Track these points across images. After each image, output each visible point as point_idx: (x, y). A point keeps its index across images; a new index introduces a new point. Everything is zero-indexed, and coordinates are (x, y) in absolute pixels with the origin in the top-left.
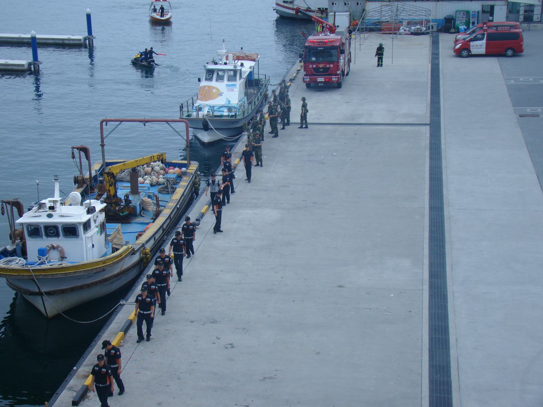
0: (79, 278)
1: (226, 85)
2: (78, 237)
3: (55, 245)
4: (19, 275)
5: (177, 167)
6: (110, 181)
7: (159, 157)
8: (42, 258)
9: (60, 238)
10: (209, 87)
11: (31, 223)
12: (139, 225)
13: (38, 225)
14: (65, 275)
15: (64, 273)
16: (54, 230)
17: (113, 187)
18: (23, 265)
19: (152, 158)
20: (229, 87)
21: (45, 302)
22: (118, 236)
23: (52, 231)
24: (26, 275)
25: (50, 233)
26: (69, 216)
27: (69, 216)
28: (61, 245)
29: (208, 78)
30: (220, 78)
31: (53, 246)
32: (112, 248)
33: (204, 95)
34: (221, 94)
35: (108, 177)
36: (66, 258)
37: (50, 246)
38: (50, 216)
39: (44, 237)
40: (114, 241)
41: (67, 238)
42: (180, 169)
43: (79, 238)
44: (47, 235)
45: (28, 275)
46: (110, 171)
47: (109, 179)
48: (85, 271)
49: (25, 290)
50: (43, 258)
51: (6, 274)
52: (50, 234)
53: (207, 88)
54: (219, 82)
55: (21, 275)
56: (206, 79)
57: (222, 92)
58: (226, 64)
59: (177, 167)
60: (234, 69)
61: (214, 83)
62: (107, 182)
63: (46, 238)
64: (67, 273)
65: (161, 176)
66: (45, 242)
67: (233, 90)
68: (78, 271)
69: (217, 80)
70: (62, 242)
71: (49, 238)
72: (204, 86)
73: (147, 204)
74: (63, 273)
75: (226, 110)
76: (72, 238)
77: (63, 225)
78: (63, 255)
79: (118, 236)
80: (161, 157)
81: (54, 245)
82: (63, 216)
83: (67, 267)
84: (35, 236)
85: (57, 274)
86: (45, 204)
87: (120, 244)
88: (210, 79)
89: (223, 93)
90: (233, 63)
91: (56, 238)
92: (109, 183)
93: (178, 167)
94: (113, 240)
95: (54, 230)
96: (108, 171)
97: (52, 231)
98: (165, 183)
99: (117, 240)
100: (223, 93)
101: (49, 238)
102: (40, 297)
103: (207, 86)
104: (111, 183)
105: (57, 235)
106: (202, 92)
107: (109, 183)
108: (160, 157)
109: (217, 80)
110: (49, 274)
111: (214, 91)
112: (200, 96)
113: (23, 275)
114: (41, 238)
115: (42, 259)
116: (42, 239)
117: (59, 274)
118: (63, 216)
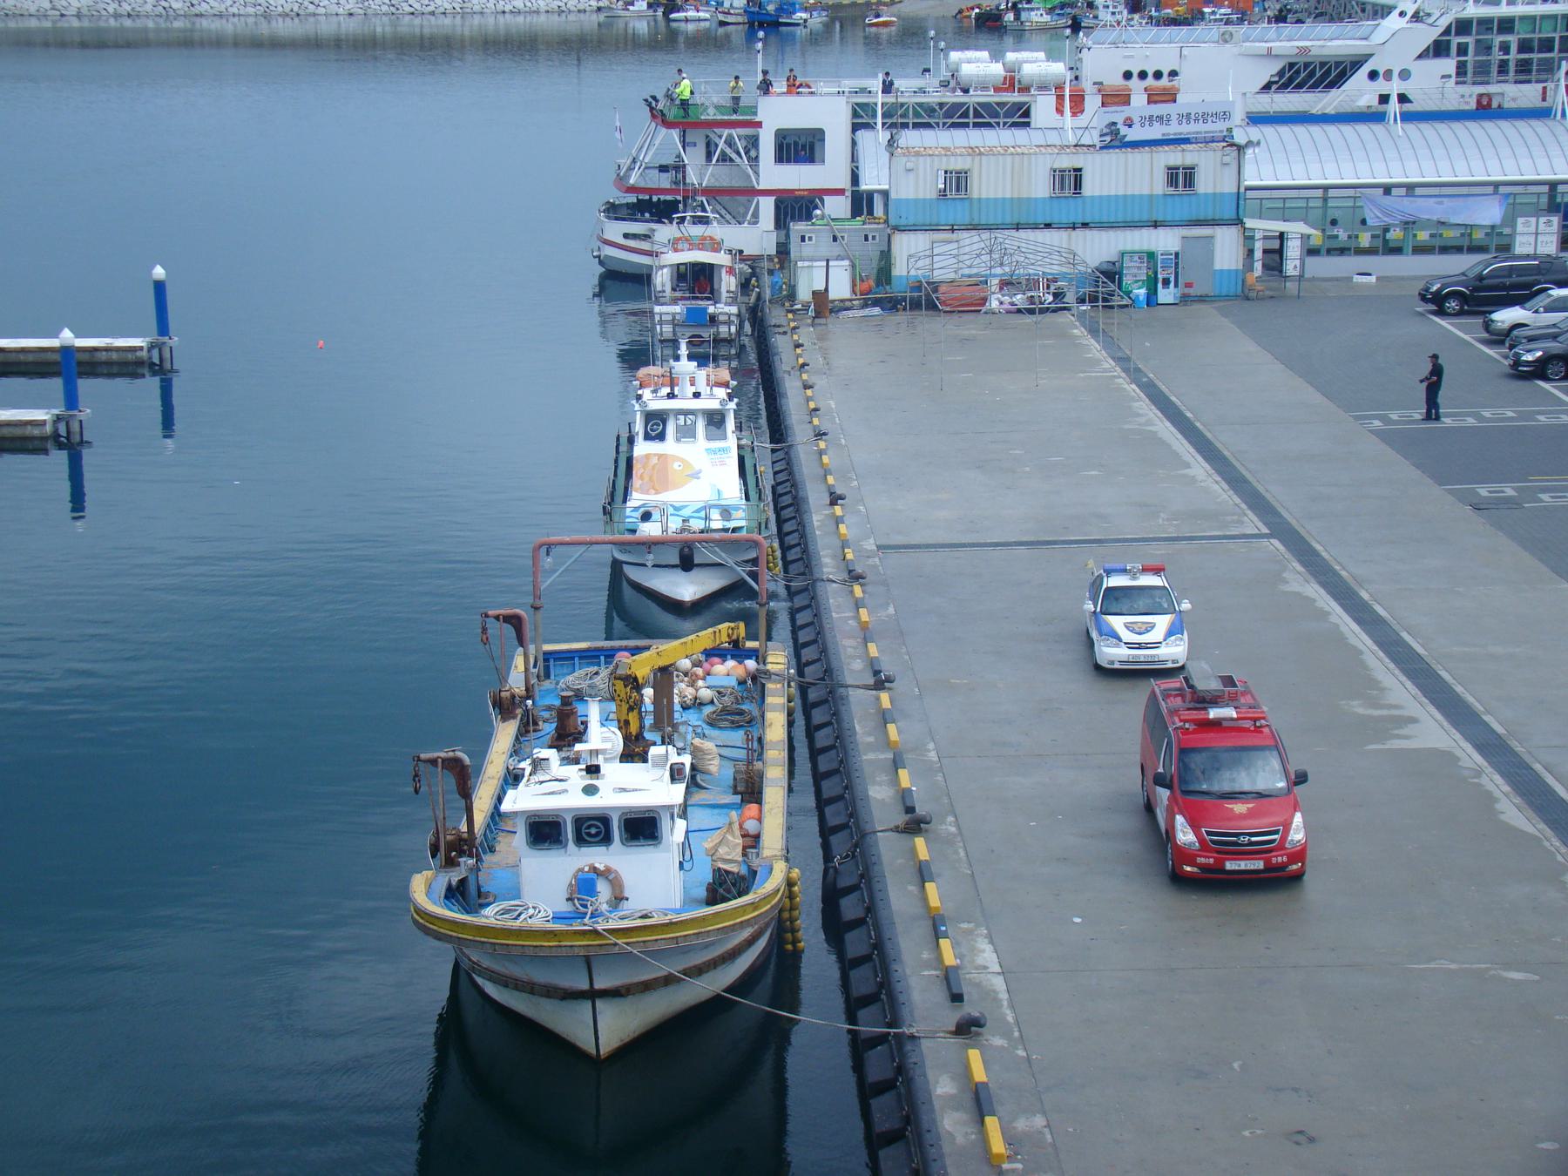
0: (706, 946)
1: (707, 450)
2: (660, 843)
3: (601, 867)
4: (560, 946)
5: (729, 657)
6: (630, 697)
7: (730, 631)
8: (588, 901)
9: (612, 847)
10: (660, 456)
11: (538, 811)
12: (708, 811)
13: (557, 816)
14: (675, 941)
15: (673, 938)
16: (597, 827)
17: (636, 711)
18: (548, 921)
19: (717, 634)
20: (713, 456)
21: (599, 1018)
22: (730, 838)
23: (593, 831)
24: (580, 946)
25: (589, 834)
26: (640, 790)
27: (640, 790)
28: (614, 866)
29: (653, 434)
30: (687, 433)
31: (595, 868)
32: (714, 870)
33: (651, 477)
34: (695, 475)
35: (626, 686)
36: (627, 899)
37: (586, 869)
38: (590, 790)
39: (571, 844)
40: (722, 851)
41: (631, 846)
42: (740, 663)
43: (661, 846)
44: (581, 840)
45: (584, 946)
46: (629, 673)
47: (627, 693)
48: (718, 929)
49: (545, 986)
50: (593, 899)
51: (523, 946)
52: (588, 839)
53: (655, 460)
54: (685, 442)
55: (565, 946)
56: (647, 437)
57: (697, 468)
58: (697, 395)
59: (729, 657)
60: (720, 407)
61: (670, 446)
62: (621, 701)
63: (577, 849)
64: (680, 936)
65: (700, 683)
66: (570, 861)
67: (723, 464)
68: (703, 930)
69: (678, 440)
70: (618, 857)
71: (585, 850)
72: (648, 456)
73: (705, 756)
74: (669, 938)
75: (715, 514)
76: (643, 846)
77: (623, 813)
78: (622, 892)
79: (730, 838)
80: (735, 631)
81: (597, 865)
82: (624, 790)
83: (681, 921)
84: (547, 844)
85: (656, 940)
86: (547, 759)
87: (735, 858)
88: (661, 437)
89: (700, 471)
90: (709, 393)
91: (603, 849)
92: (628, 702)
93: (732, 658)
94: (717, 850)
95: (597, 827)
96: (624, 672)
97: (593, 831)
98: (715, 700)
99: (726, 849)
100: (700, 471)
101: (582, 849)
102: (588, 1004)
103: (655, 455)
104: (632, 704)
105: (606, 839)
106: (642, 471)
107: (628, 702)
108: (733, 634)
109: (678, 440)
110: (638, 942)
111: (676, 465)
112: (640, 482)
113: (571, 946)
114: (563, 850)
115: (589, 903)
116: (566, 852)
117: (661, 939)
118: (624, 790)
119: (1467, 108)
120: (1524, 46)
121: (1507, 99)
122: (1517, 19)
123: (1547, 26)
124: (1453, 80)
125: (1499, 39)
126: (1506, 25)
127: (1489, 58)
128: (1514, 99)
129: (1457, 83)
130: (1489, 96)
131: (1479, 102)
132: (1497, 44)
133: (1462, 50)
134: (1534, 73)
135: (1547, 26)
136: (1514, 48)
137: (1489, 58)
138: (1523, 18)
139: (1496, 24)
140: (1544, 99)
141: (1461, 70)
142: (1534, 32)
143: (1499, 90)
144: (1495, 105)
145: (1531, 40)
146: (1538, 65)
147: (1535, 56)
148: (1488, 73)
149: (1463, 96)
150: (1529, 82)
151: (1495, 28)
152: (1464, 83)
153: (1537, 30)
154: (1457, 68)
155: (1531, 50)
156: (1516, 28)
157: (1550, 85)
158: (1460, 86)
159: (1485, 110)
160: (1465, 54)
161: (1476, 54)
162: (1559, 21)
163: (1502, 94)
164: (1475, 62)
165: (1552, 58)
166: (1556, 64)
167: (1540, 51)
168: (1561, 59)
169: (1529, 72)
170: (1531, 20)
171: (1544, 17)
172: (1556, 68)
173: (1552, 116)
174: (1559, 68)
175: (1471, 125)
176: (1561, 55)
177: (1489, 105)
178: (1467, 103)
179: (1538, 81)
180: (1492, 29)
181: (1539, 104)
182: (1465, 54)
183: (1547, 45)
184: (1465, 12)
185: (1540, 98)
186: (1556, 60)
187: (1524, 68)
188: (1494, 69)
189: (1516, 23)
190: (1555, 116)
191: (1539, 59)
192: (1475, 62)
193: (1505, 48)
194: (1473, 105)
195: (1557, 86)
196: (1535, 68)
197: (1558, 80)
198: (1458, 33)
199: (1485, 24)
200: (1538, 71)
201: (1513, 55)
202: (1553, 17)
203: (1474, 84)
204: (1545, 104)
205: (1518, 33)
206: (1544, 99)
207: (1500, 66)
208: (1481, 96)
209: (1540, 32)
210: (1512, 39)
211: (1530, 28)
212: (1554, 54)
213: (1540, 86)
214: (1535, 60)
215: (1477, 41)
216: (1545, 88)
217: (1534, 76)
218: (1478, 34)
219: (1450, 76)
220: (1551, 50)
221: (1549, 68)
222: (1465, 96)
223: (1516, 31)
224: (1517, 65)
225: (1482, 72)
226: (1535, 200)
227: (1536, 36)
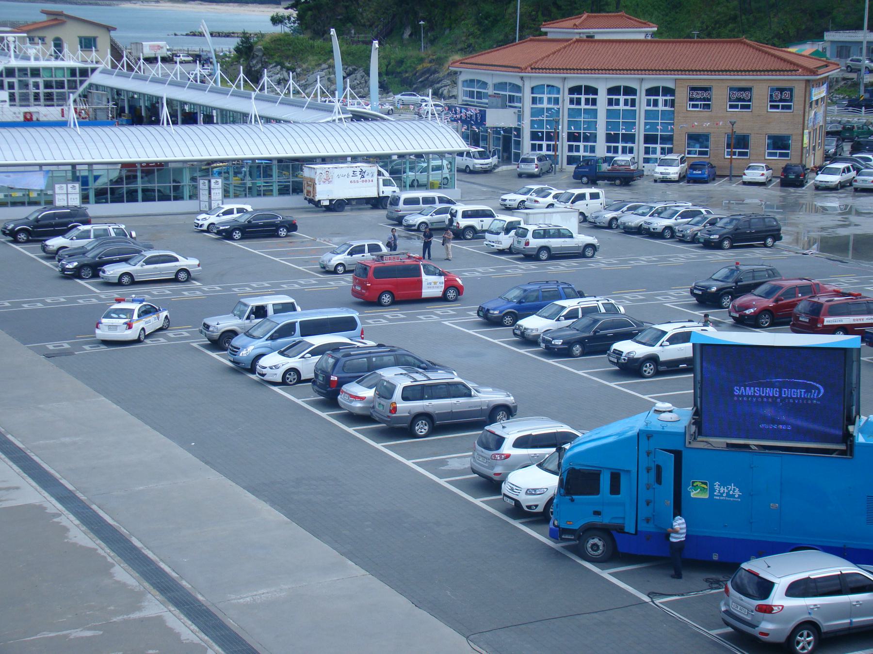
119: (18, 120)
120: (48, 85)
121: (41, 115)
122: (41, 69)
123: (59, 73)
124: (8, 103)
125: (31, 80)
126: (36, 72)
127: (28, 91)
128: (45, 116)
129: (11, 105)
130: (30, 113)
131: (25, 117)
132: (31, 83)
133: (11, 86)
134: (55, 100)
135: (59, 73)
136: (42, 86)
137: (28, 91)
138: (45, 69)
139: (29, 71)
140: (63, 116)
141: (12, 97)
142: (52, 76)
143: (36, 110)
144: (34, 118)
145: (51, 82)
146: (57, 96)
147: (54, 91)
148: (28, 100)
149: (15, 113)
150: (53, 106)
151: (29, 74)
152: (15, 105)
153: (54, 76)
154: (10, 96)
155: (52, 87)
156: (41, 74)
157: (65, 108)
158: (12, 107)
159: (29, 121)
160: (13, 88)
161: (20, 88)
162: (65, 71)
163: (38, 113)
164: (20, 93)
165: (65, 92)
166: (67, 95)
167: (57, 88)
168: (69, 93)
169: (52, 100)
170: (49, 69)
171: (57, 69)
172: (67, 98)
173: (68, 126)
174: (69, 98)
175: (21, 130)
176: (69, 91)
177: (31, 119)
178: (18, 117)
179: (58, 105)
180: (27, 74)
181: (60, 118)
182: (13, 88)
183: (60, 85)
184: (10, 64)
185: (60, 115)
186: (67, 93)
187: (49, 97)
188: (32, 98)
189: (41, 71)
190: (70, 125)
191: (57, 93)
192: (20, 93)
193: (37, 86)
194: (22, 119)
195: (69, 108)
196: (55, 97)
197: (70, 105)
198: (8, 76)
199: (23, 71)
200: (57, 99)
201: (42, 90)
202: (62, 69)
203: (21, 106)
204: (64, 119)
205: (43, 77)
206: (63, 116)
207: (35, 96)
208: (26, 113)
209: (56, 77)
210: (40, 81)
211: (49, 75)
212: (66, 90)
213: (59, 108)
214: (55, 93)
215: (20, 81)
216: (63, 109)
217: (55, 103)
218: (19, 76)
219: (5, 101)
220: (63, 87)
221: (63, 98)
222: (16, 113)
223: (41, 76)
224: (44, 96)
225: (25, 99)
226: (65, 175)
227: (54, 79)
